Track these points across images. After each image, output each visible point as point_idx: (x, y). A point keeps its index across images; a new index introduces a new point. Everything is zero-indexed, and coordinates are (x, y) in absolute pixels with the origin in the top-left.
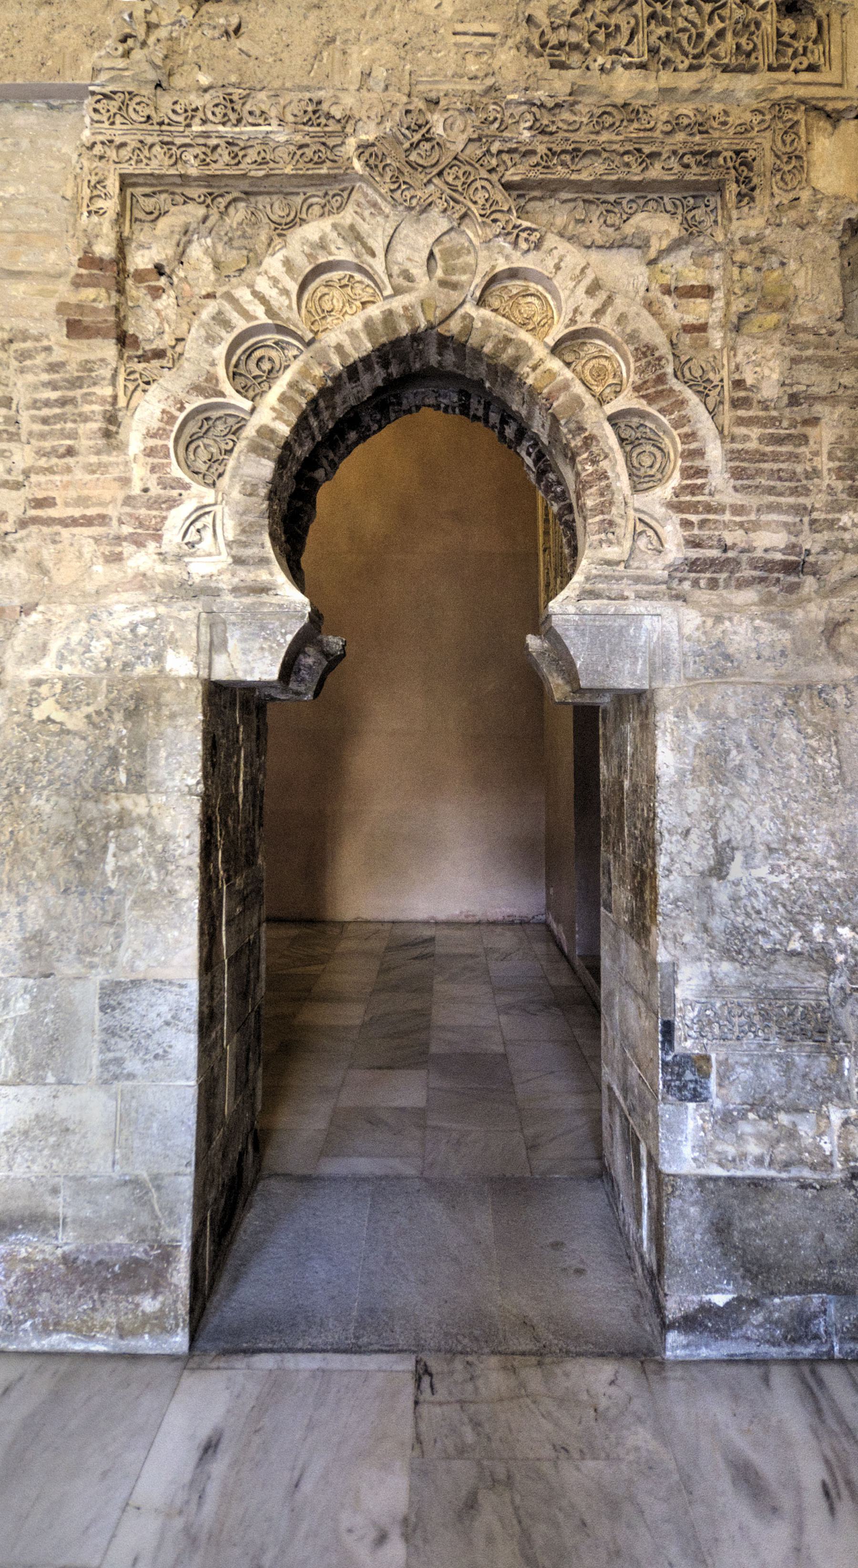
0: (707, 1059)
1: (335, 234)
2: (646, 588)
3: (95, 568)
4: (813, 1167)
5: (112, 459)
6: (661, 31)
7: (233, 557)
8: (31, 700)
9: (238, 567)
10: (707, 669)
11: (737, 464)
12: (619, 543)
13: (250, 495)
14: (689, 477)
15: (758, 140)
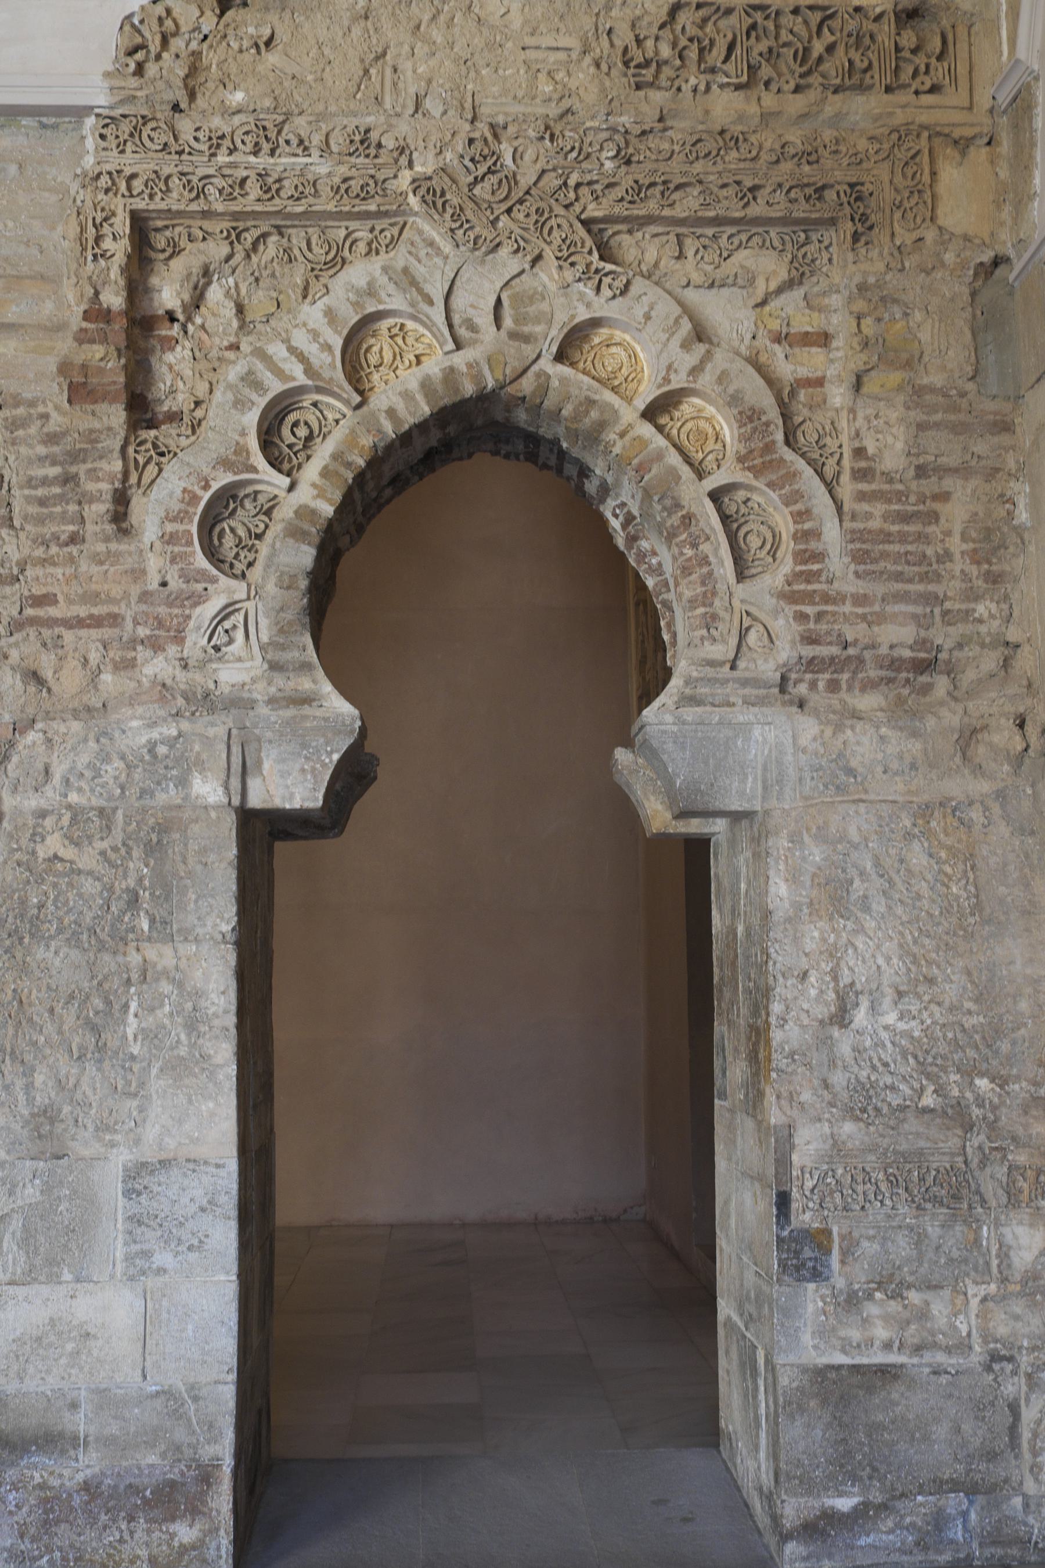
0: (827, 1233)
1: (386, 279)
2: (755, 692)
3: (103, 676)
4: (948, 1350)
5: (123, 547)
6: (763, 46)
7: (270, 662)
8: (34, 834)
9: (275, 674)
10: (826, 786)
11: (858, 546)
12: (725, 642)
13: (288, 588)
14: (805, 562)
15: (875, 172)
